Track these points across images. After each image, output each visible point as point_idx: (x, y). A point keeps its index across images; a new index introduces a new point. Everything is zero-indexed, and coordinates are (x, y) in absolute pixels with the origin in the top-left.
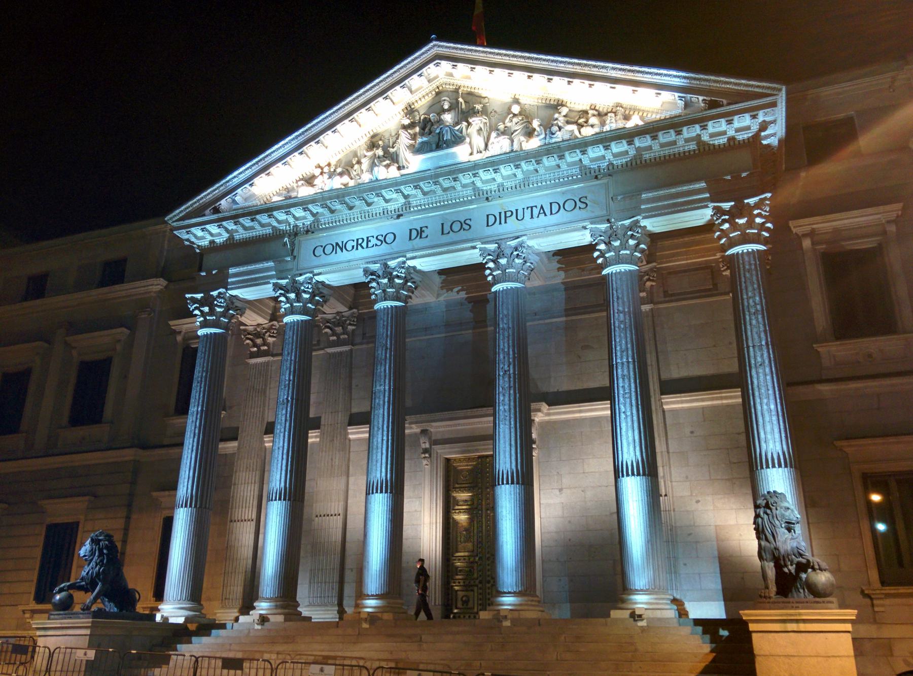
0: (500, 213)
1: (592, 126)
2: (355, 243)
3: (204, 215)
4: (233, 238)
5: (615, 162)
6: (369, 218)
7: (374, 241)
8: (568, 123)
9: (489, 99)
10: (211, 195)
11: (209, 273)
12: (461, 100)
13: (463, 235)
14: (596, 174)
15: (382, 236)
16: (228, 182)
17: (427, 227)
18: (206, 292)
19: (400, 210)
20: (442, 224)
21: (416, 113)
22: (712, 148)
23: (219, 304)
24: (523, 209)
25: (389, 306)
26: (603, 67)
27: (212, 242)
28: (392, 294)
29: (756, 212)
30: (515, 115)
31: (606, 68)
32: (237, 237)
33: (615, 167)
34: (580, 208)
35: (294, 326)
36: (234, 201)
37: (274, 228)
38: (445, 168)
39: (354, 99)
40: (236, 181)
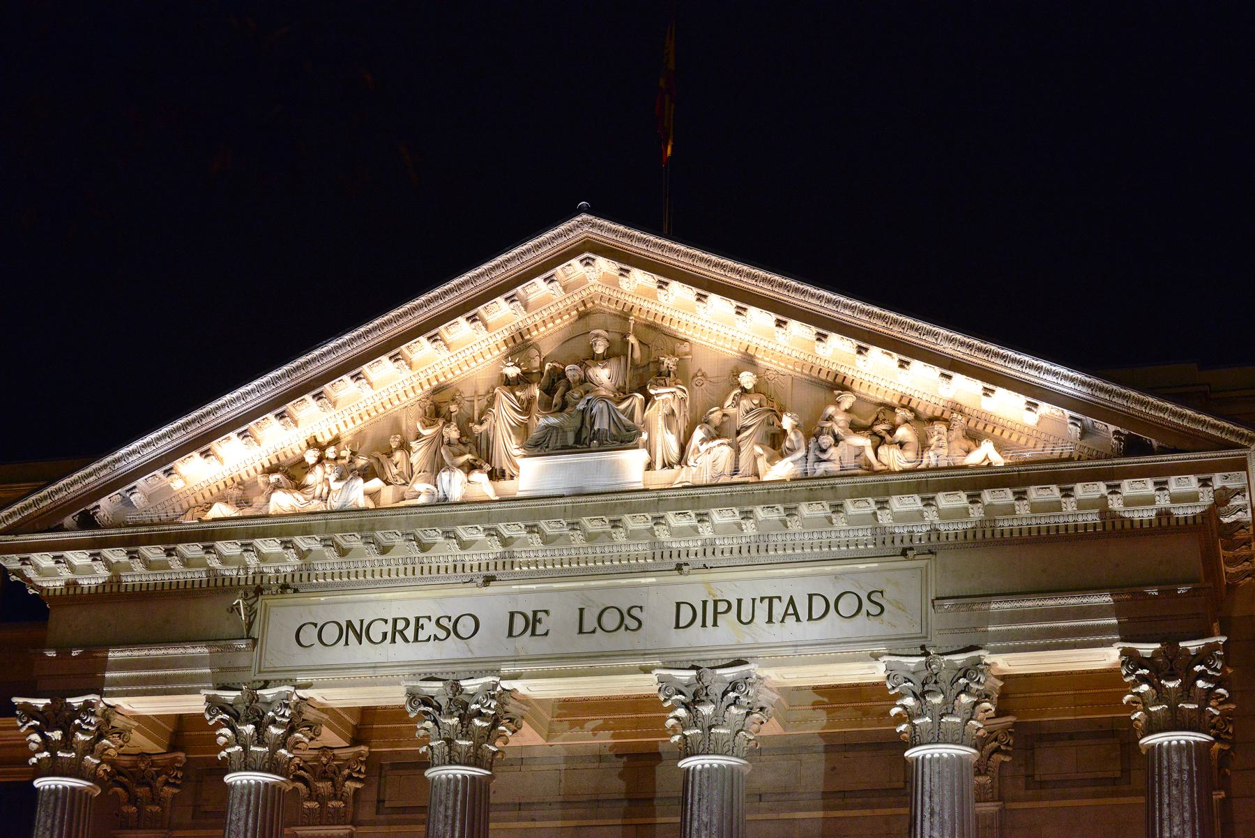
0: (705, 603)
1: (902, 445)
2: (388, 628)
3: (60, 529)
4: (119, 582)
5: (942, 528)
6: (420, 576)
7: (430, 629)
8: (855, 428)
9: (691, 344)
10: (80, 485)
11: (63, 651)
12: (632, 339)
13: (624, 640)
15: (450, 618)
16: (118, 460)
17: (546, 612)
18: (58, 695)
19: (492, 567)
20: (581, 610)
21: (534, 352)
22: (1127, 525)
23: (85, 727)
24: (754, 600)
25: (459, 776)
26: (929, 333)
27: (71, 584)
28: (464, 750)
29: (1198, 668)
30: (745, 391)
31: (935, 335)
32: (128, 579)
33: (943, 538)
34: (868, 614)
35: (249, 794)
36: (127, 502)
37: (210, 570)
38: (594, 498)
39: (405, 314)
40: (135, 461)
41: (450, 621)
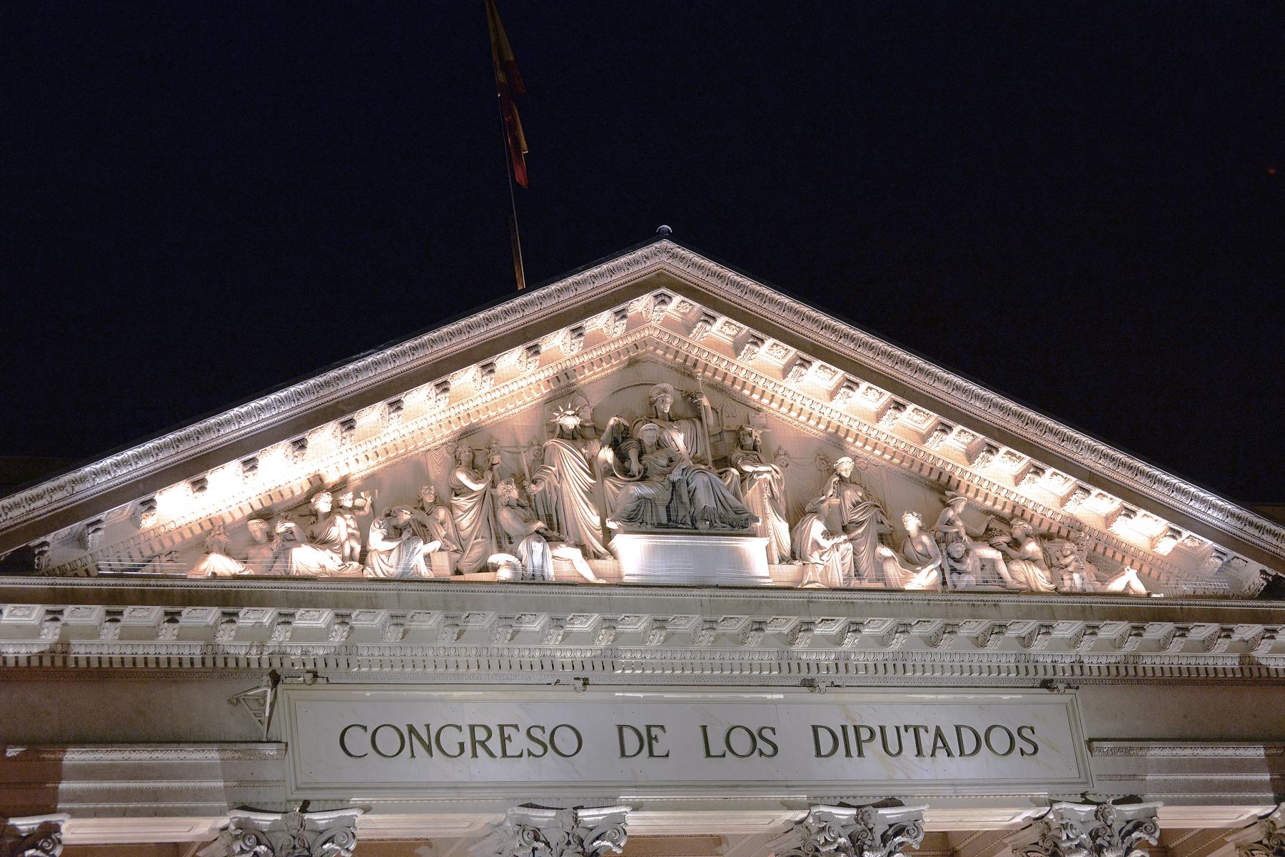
0: (844, 728)
2: (466, 737)
7: (519, 742)
10: (23, 510)
13: (757, 767)
14: (1049, 676)
17: (662, 727)
19: (588, 666)
20: (704, 728)
33: (1086, 671)
34: (1022, 752)
38: (736, 592)
40: (103, 483)
41: (544, 732)
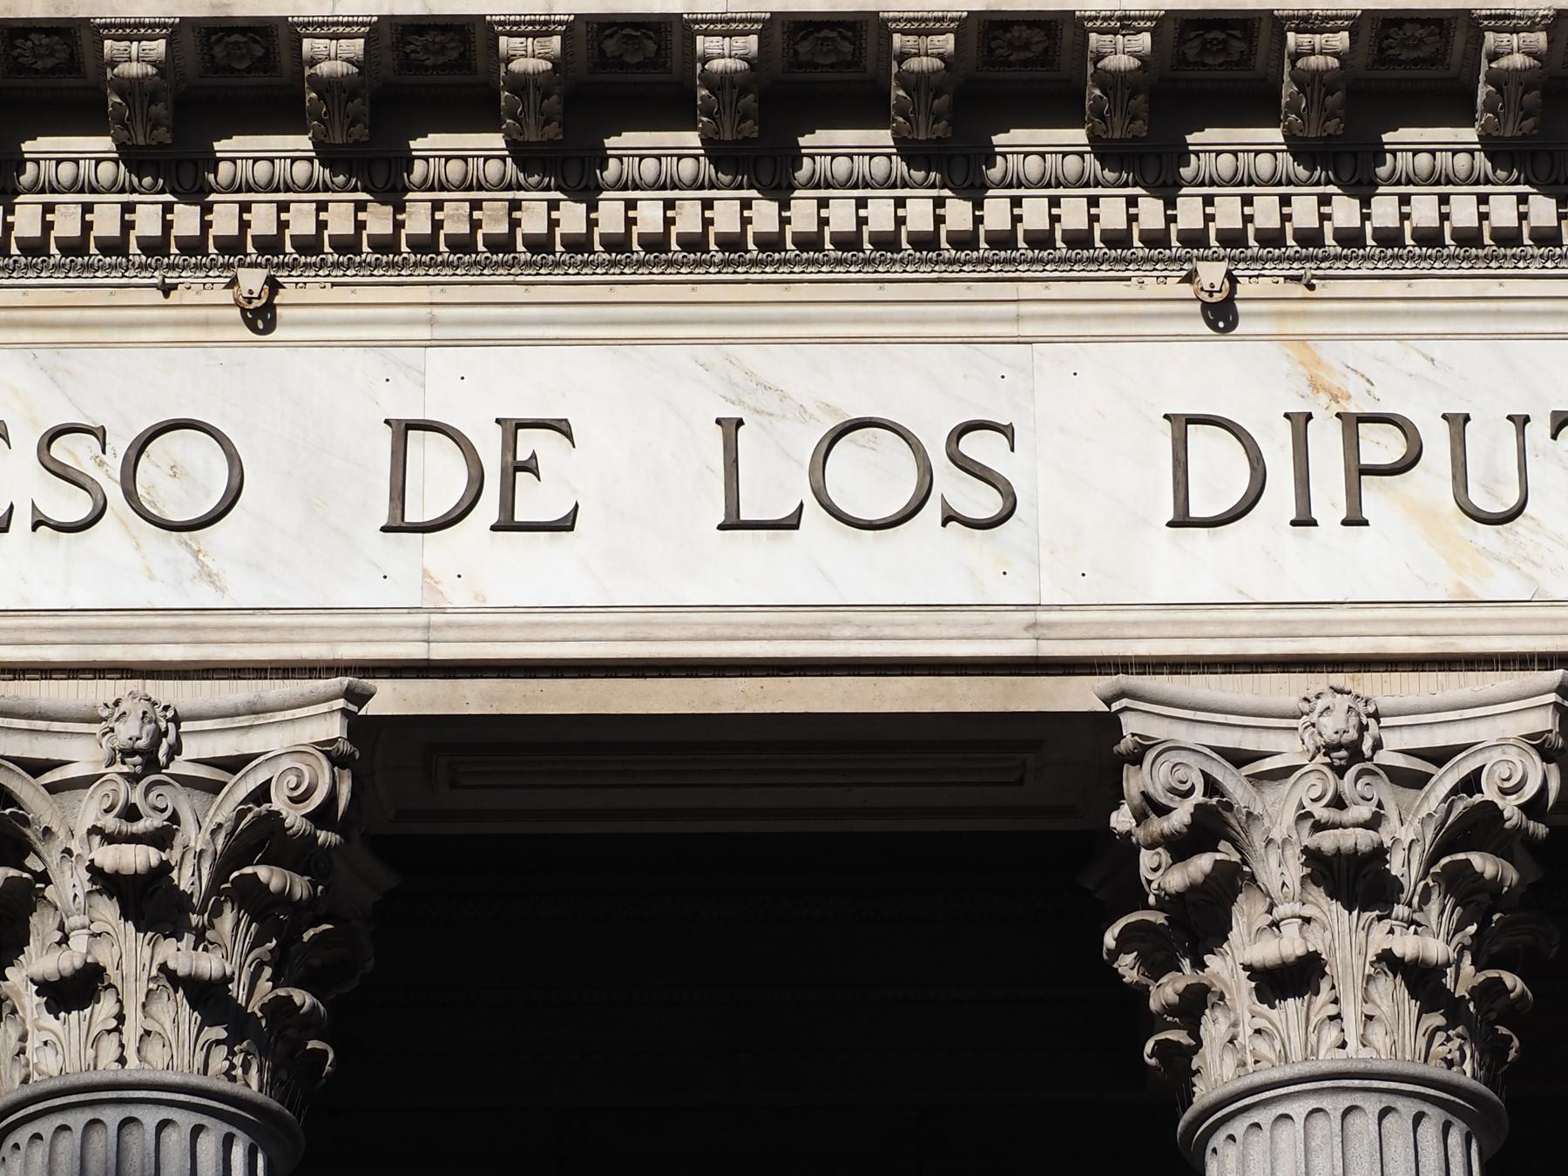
0: (1300, 422)
17: (562, 428)
24: (1521, 422)
